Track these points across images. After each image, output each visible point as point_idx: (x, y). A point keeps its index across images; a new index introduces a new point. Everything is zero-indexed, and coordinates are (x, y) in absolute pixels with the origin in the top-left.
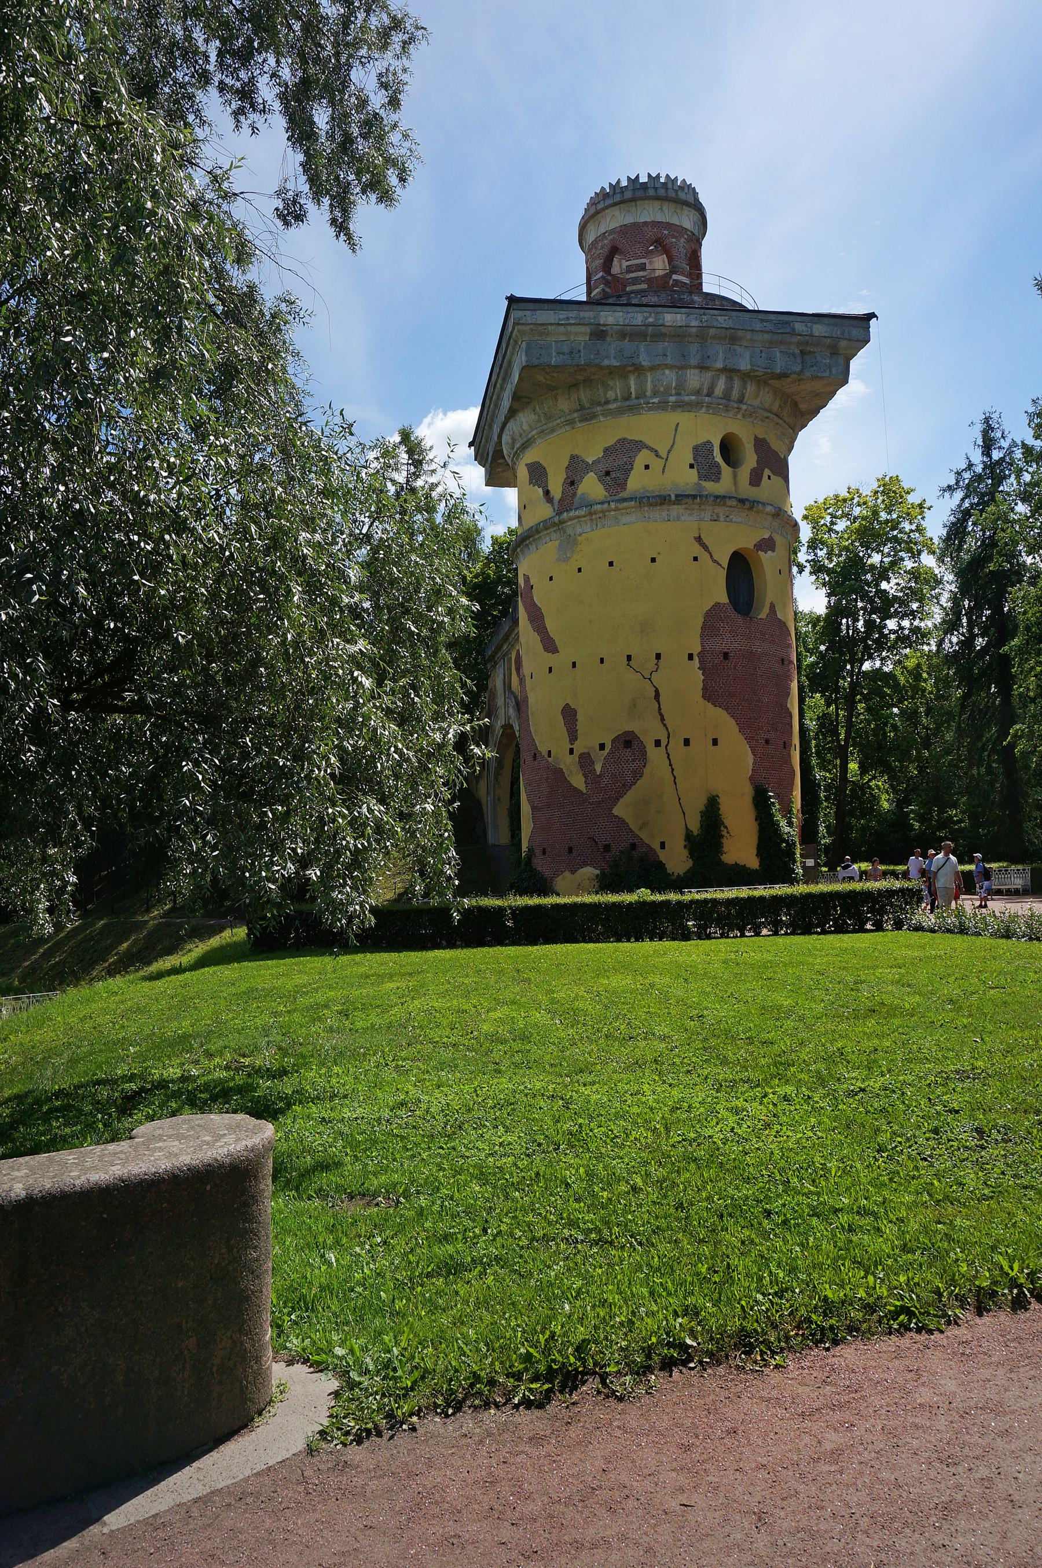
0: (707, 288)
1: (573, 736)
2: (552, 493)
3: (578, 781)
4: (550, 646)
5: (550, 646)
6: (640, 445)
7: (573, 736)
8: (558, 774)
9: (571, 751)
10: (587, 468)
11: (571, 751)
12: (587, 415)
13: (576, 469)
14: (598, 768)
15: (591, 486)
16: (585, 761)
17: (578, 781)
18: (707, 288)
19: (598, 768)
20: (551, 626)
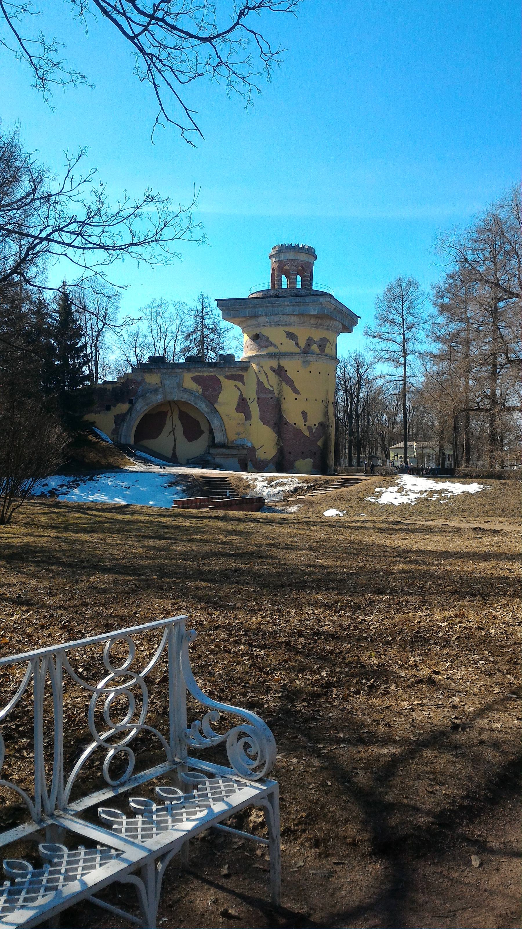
0: (314, 288)
1: (306, 420)
2: (300, 345)
3: (307, 434)
4: (296, 391)
5: (296, 391)
6: (328, 341)
7: (306, 420)
8: (299, 432)
9: (305, 425)
10: (314, 342)
11: (305, 425)
12: (317, 326)
13: (310, 342)
14: (314, 431)
15: (315, 348)
16: (310, 428)
17: (307, 434)
18: (314, 288)
19: (314, 431)
20: (296, 384)
